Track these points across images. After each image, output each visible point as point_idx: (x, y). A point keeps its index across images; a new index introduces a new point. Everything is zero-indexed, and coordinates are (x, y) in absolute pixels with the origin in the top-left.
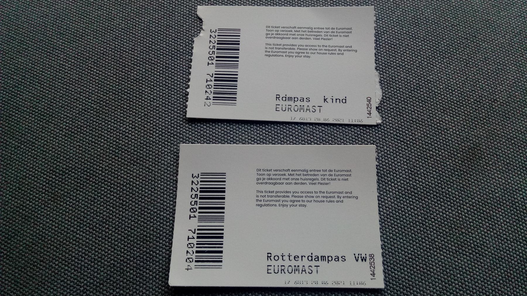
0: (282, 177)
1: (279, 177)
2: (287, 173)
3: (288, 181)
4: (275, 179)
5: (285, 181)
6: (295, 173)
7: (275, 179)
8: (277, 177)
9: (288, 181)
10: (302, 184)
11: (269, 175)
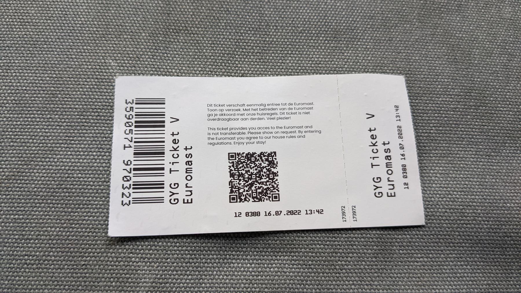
0: (236, 112)
1: (233, 112)
2: (241, 108)
3: (243, 117)
4: (229, 115)
5: (240, 117)
7: (229, 115)
8: (231, 112)
9: (243, 117)
10: (259, 119)
11: (222, 110)
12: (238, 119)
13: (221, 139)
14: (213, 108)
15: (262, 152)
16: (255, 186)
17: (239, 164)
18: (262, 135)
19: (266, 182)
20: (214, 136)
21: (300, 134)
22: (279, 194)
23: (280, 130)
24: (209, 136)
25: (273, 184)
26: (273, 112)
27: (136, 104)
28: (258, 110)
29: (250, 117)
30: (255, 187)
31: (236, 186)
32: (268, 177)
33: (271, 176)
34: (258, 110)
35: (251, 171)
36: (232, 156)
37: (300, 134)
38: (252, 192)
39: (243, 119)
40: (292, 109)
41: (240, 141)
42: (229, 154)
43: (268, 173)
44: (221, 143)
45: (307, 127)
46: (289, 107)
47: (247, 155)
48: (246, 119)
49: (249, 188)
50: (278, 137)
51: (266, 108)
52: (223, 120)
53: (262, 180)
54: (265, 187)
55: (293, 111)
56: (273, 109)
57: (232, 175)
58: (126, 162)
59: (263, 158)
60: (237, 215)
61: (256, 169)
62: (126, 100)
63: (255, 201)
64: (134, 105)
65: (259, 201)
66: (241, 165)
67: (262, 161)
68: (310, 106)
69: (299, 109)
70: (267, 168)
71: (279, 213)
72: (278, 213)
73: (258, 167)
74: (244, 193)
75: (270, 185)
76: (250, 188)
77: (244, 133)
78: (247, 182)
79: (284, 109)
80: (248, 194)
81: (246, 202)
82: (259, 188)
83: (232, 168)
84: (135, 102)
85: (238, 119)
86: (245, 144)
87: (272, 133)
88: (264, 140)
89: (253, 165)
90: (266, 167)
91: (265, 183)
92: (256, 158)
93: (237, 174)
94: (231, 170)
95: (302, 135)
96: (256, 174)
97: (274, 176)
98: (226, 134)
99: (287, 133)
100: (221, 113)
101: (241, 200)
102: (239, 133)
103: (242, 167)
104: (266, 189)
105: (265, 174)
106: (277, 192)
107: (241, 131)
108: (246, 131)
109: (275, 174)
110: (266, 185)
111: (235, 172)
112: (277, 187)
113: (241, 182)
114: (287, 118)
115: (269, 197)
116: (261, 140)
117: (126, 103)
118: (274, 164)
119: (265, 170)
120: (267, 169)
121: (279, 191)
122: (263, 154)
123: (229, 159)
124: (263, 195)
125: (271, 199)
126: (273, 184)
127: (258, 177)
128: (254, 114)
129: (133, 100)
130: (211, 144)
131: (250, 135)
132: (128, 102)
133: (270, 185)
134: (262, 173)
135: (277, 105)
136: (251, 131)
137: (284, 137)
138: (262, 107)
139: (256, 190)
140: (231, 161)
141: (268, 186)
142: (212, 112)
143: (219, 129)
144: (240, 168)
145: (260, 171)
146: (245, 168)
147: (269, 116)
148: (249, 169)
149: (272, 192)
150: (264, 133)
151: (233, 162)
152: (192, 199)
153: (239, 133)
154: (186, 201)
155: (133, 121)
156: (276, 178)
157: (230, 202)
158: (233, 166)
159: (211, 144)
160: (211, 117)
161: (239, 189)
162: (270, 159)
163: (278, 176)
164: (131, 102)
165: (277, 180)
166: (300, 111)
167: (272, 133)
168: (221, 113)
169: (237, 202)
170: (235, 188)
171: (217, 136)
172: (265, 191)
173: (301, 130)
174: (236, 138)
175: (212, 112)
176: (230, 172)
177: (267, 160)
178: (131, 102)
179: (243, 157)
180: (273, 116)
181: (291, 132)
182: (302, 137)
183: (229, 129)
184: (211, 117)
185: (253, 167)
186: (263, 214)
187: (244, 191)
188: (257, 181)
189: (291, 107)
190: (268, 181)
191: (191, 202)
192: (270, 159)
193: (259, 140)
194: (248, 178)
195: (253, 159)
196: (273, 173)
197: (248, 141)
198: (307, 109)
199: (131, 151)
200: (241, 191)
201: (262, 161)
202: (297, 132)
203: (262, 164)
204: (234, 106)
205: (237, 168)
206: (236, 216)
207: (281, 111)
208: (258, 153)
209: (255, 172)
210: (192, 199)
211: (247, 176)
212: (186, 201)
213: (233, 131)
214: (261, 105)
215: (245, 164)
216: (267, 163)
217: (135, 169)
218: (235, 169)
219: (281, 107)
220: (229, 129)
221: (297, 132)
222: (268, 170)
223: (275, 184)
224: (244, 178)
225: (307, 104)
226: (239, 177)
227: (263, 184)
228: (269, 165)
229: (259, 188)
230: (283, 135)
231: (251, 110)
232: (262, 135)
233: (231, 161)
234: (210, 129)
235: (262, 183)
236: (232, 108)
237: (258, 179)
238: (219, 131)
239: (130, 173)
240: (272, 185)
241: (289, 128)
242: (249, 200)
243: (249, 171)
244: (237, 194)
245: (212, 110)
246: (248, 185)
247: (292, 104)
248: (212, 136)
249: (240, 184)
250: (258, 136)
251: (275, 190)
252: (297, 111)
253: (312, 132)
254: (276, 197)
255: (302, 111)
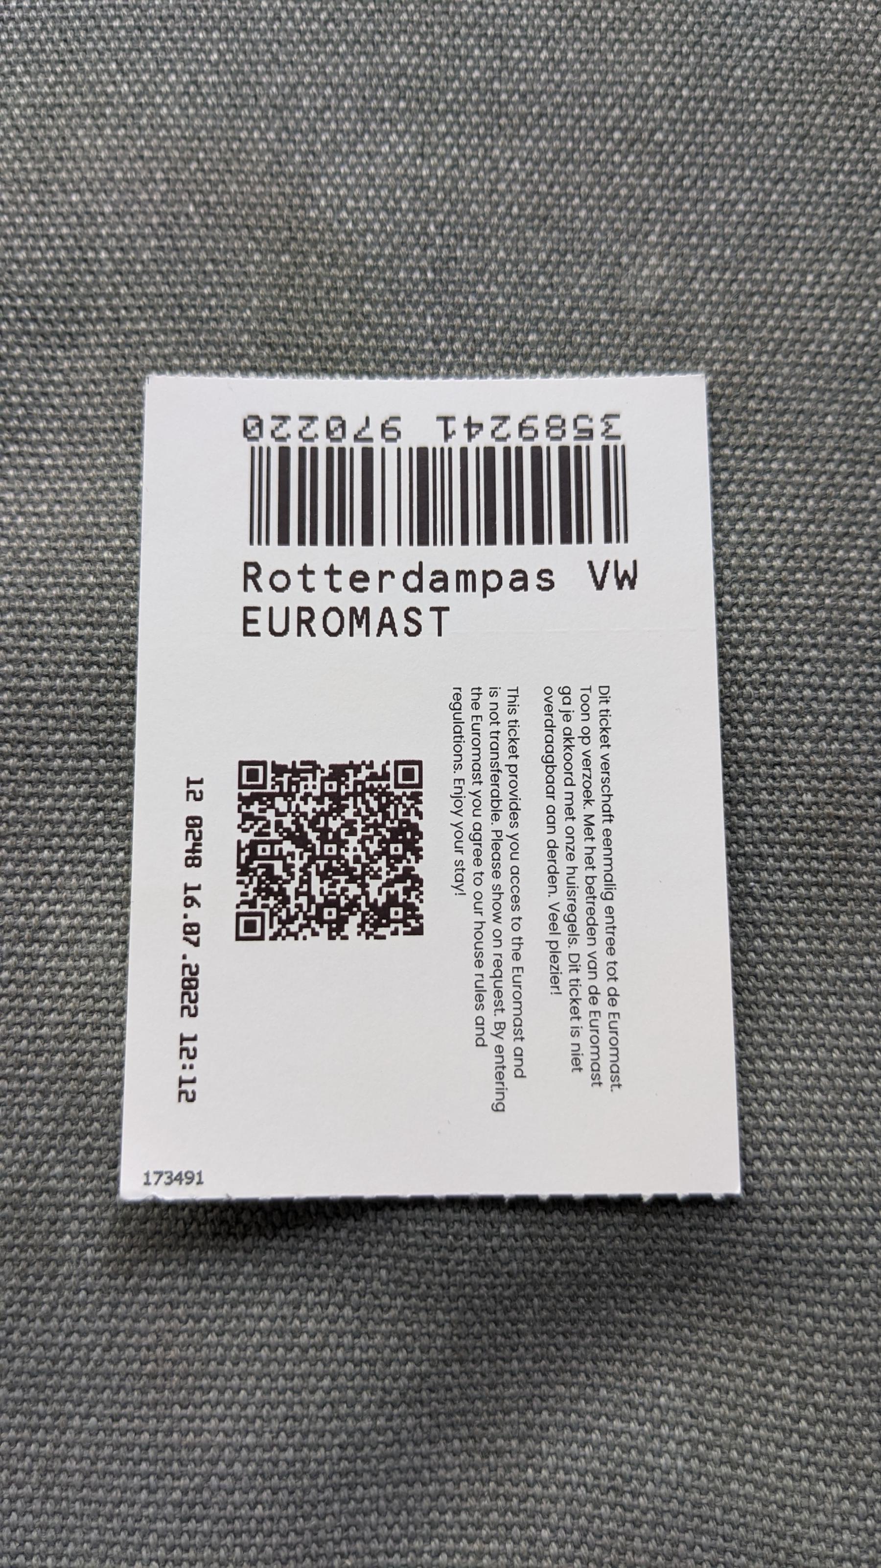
0: (578, 791)
1: (578, 779)
2: (596, 809)
3: (560, 814)
4: (568, 762)
5: (560, 803)
6: (598, 842)
7: (568, 762)
9: (560, 814)
10: (553, 875)
11: (585, 736)
12: (551, 795)
13: (476, 732)
14: (595, 707)
15: (421, 882)
16: (297, 851)
17: (378, 799)
18: (488, 881)
19: (308, 893)
20: (485, 710)
21: (489, 1028)
22: (261, 938)
23: (507, 950)
24: (485, 691)
25: (301, 920)
26: (582, 927)
27: (606, 449)
28: (590, 872)
29: (561, 839)
30: (292, 855)
31: (297, 784)
32: (328, 903)
33: (331, 914)
34: (590, 872)
35: (353, 841)
36: (408, 775)
37: (489, 1028)
38: (273, 843)
39: (551, 814)
40: (594, 1000)
41: (468, 800)
42: (419, 763)
43: (343, 902)
44: (459, 735)
45: (519, 1057)
46: (603, 991)
47: (415, 829)
48: (551, 825)
49: (287, 830)
50: (479, 941)
51: (598, 901)
52: (549, 743)
53: (315, 880)
54: (290, 890)
55: (585, 1007)
56: (592, 928)
57: (338, 772)
58: (392, 424)
59: (399, 887)
60: (192, 787)
61: (357, 859)
62: (617, 416)
63: (240, 850)
64: (596, 445)
65: (239, 865)
66: (374, 805)
67: (389, 883)
68: (605, 1075)
69: (594, 1029)
70: (362, 901)
71: (194, 938)
72: (191, 931)
73: (364, 866)
74: (270, 815)
75: (299, 906)
76: (290, 836)
77: (496, 816)
78: (313, 824)
79: (593, 970)
80: (267, 826)
81: (239, 818)
82: (287, 868)
83: (365, 773)
84: (611, 443)
85: (551, 795)
86: (456, 819)
87: (497, 919)
88: (469, 887)
89: (373, 848)
90: (366, 894)
91: (305, 888)
92: (399, 859)
93: (343, 791)
94: (357, 769)
95: (487, 1037)
96: (339, 857)
97: (330, 923)
98: (495, 750)
99: (497, 978)
100: (576, 733)
101: (247, 801)
102: (496, 799)
103: (369, 809)
104: (282, 891)
105: (338, 890)
106: (269, 933)
107: (505, 806)
108: (504, 823)
109: (337, 929)
110: (298, 894)
111: (351, 783)
112: (289, 934)
113: (312, 804)
114: (555, 980)
115: (252, 904)
116: (468, 876)
117: (607, 416)
118: (376, 925)
119: (354, 890)
120: (357, 897)
121: (273, 938)
122: (413, 888)
123: (397, 763)
124: (260, 882)
125: (245, 908)
126: (301, 920)
127: (328, 867)
128: (571, 856)
129: (618, 437)
130: (457, 697)
131: (488, 837)
132: (611, 421)
133: (299, 906)
134: (343, 878)
135: (611, 942)
136: (506, 843)
137: (479, 964)
138: (599, 887)
139: (281, 857)
140: (390, 769)
141: (293, 902)
142: (576, 705)
143: (512, 728)
144: (365, 802)
145: (349, 871)
146: (365, 819)
147: (563, 910)
148: (360, 834)
149: (272, 914)
150: (497, 891)
151: (385, 776)
152: (257, 634)
153: (496, 799)
154: (251, 615)
155: (542, 441)
156: (324, 931)
157: (241, 764)
158: (373, 777)
159: (457, 697)
160: (557, 699)
161: (289, 796)
162: (397, 913)
163: (331, 938)
164: (611, 432)
165: (315, 934)
166: (586, 1033)
167: (497, 919)
168: (576, 733)
169: (241, 786)
170: (291, 782)
171: (487, 720)
172: (276, 888)
173: (508, 1033)
174: (477, 787)
175: (576, 705)
176: (351, 765)
177: (392, 900)
178: (611, 432)
179: (407, 814)
180: (562, 926)
181: (498, 992)
182: (479, 1037)
183: (513, 761)
184: (557, 699)
185: (365, 849)
186: (193, 876)
187: (278, 814)
188: (312, 860)
189: (603, 998)
190: (311, 900)
191: (246, 633)
192: (397, 913)
193: (470, 869)
194: (326, 829)
195: (397, 849)
196: (341, 922)
197: (468, 830)
198: (595, 1062)
199: (433, 439)
200: (281, 804)
201: (389, 883)
202: (501, 1017)
203: (379, 883)
204: (605, 782)
205: (365, 790)
206: (189, 782)
207: (584, 961)
208: (420, 870)
209: (349, 856)
210: (257, 634)
211: (335, 824)
212: (251, 615)
213: (505, 778)
214: (610, 884)
215: (379, 818)
216: (382, 900)
217: (367, 454)
218: (362, 783)
219: (602, 959)
220: (513, 761)
221: (501, 1017)
222: (353, 904)
223: (301, 927)
224: (327, 815)
225: (614, 1063)
226: (331, 796)
227: (302, 881)
228: (373, 906)
229: (287, 868)
230: (488, 959)
231: (589, 843)
232: (488, 881)
233: (390, 769)
234: (514, 694)
235: (306, 880)
236: (597, 774)
237: (322, 863)
238: (504, 728)
239: (356, 438)
240: (296, 917)
241: (517, 984)
242: (245, 831)
243: (353, 832)
244: (269, 790)
245: (585, 703)
246: (300, 827)
247: (613, 1002)
248: (485, 701)
249: (304, 799)
250: (487, 866)
251: (277, 926)
252: (584, 1022)
253: (500, 1077)
254: (250, 926)
255: (584, 1039)
